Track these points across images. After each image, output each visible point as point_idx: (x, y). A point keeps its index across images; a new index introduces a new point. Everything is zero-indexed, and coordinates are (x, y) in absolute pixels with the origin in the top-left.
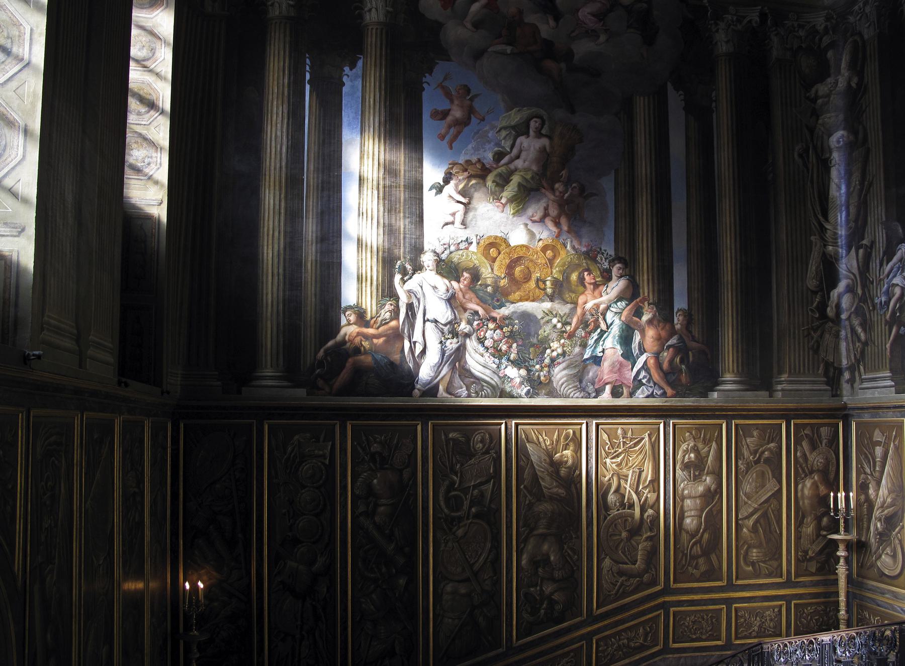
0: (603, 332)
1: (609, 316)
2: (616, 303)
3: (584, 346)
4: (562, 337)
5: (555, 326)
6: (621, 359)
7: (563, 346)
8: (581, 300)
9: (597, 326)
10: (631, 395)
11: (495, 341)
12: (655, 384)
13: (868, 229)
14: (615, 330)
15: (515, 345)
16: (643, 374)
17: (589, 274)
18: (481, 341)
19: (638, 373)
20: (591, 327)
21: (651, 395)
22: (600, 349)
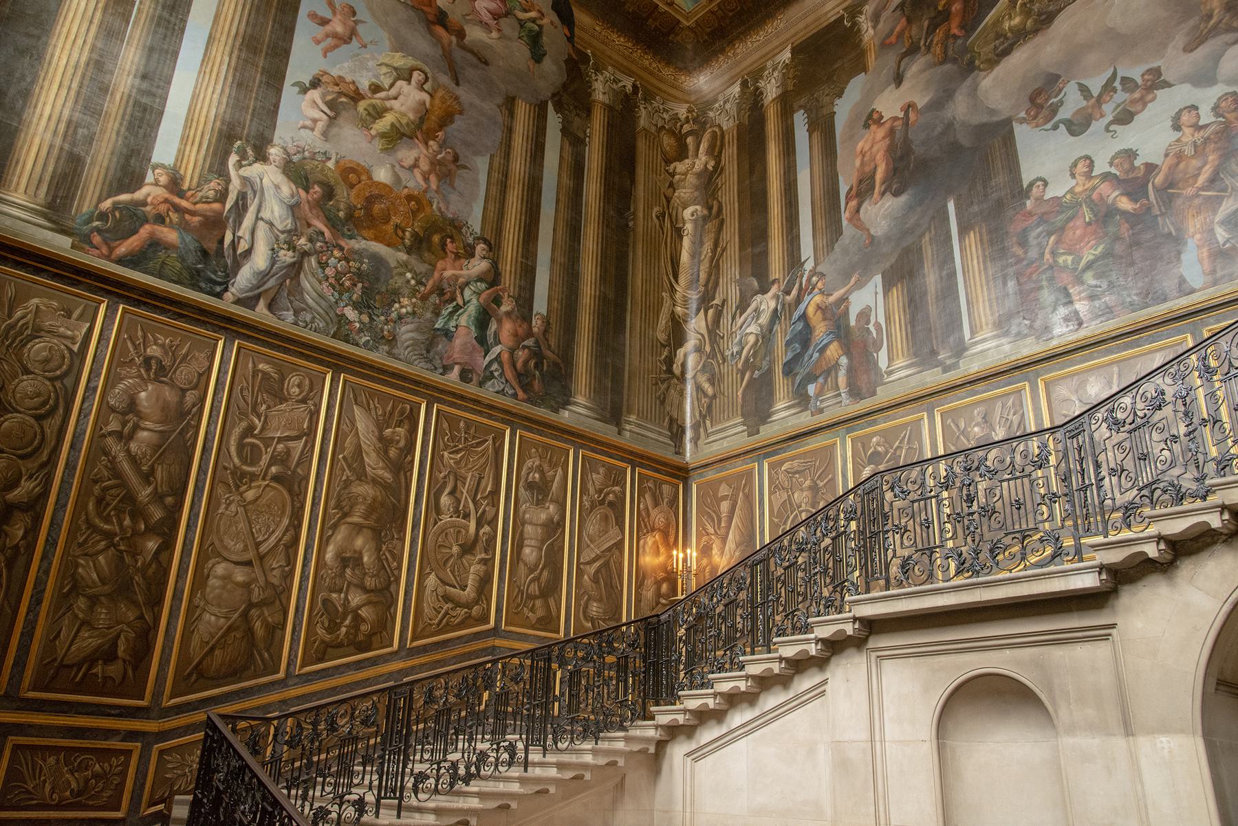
0: (458, 308)
1: (467, 293)
5: (408, 281)
8: (440, 265)
9: (453, 299)
11: (338, 272)
14: (472, 309)
15: (360, 285)
16: (495, 366)
18: (323, 265)
20: (447, 296)
21: (502, 392)
22: (453, 323)
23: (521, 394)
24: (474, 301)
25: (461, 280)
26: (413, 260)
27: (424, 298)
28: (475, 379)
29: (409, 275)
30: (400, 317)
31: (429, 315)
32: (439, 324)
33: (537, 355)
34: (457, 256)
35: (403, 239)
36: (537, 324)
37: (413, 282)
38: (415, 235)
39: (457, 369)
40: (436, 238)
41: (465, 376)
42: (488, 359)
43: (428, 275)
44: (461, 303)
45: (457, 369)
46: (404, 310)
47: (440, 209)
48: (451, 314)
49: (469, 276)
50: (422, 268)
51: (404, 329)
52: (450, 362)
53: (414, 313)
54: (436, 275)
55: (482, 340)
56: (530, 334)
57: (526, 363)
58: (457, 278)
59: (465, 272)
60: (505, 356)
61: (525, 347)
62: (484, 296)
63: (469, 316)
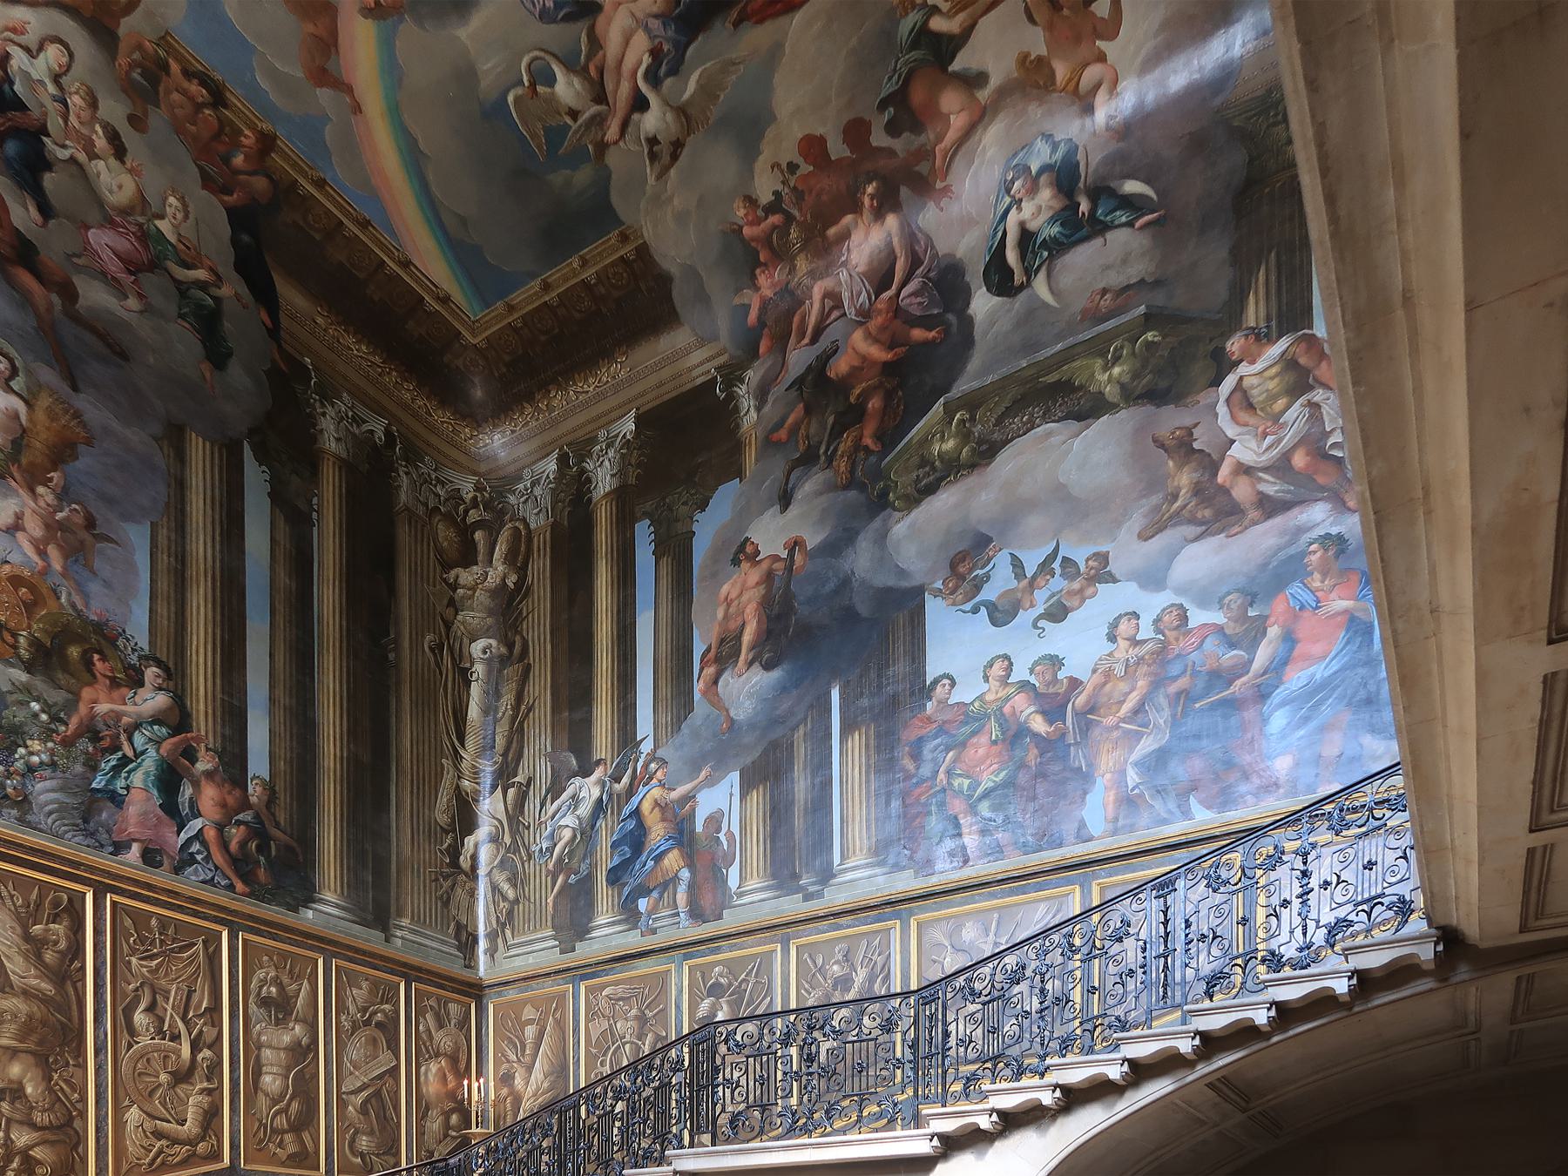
0: (125, 761)
1: (139, 739)
2: (152, 723)
3: (94, 769)
4: (49, 738)
5: (36, 716)
6: (161, 813)
7: (52, 753)
8: (87, 693)
9: (116, 748)
10: (177, 870)
12: (217, 868)
14: (149, 763)
16: (196, 847)
17: (104, 659)
19: (189, 842)
20: (106, 743)
21: (210, 882)
22: (120, 784)
23: (240, 886)
24: (152, 752)
25: (125, 720)
26: (39, 684)
27: (68, 743)
28: (166, 862)
29: (35, 706)
30: (31, 769)
31: (79, 768)
32: (98, 783)
33: (258, 832)
34: (114, 683)
35: (15, 647)
36: (255, 791)
37: (44, 717)
38: (35, 643)
39: (135, 847)
40: (74, 652)
41: (151, 857)
42: (183, 836)
43: (72, 705)
44: (130, 754)
45: (135, 847)
46: (35, 759)
47: (73, 606)
48: (117, 770)
49: (139, 715)
50: (57, 697)
51: (39, 786)
52: (123, 837)
53: (53, 765)
54: (83, 709)
55: (170, 807)
56: (245, 805)
57: (243, 844)
58: (118, 716)
59: (129, 708)
60: (211, 834)
61: (239, 823)
62: (167, 746)
63: (147, 774)
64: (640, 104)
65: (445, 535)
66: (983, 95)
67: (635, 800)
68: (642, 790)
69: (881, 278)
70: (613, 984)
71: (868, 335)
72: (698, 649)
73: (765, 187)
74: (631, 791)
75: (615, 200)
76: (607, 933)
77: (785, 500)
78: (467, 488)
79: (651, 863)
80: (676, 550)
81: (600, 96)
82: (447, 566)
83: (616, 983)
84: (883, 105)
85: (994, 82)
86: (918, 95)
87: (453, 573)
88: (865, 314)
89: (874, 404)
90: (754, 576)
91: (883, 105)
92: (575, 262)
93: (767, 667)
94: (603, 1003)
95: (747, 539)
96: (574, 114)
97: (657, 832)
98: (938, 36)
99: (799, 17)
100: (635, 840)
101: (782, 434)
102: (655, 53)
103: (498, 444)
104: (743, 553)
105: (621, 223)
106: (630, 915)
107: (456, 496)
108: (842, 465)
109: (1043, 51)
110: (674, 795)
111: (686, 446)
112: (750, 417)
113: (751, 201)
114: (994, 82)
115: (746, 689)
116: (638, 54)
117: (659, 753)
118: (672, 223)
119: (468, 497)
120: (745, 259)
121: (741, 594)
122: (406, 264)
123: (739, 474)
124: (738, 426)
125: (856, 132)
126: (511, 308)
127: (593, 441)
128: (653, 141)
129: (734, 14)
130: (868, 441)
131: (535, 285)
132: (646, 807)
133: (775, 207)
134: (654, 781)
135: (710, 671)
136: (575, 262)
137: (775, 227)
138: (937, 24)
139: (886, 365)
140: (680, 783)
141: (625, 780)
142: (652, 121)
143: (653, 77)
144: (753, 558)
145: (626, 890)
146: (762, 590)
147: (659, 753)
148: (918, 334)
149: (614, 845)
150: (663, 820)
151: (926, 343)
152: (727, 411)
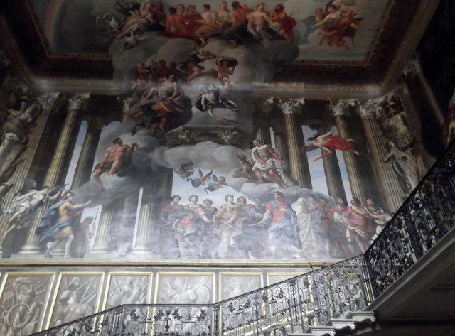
13: (12, 178)
64: (129, 35)
65: (12, 99)
66: (203, 72)
67: (57, 205)
68: (61, 202)
69: (170, 93)
70: (23, 277)
71: (164, 104)
72: (96, 163)
73: (148, 64)
74: (56, 201)
75: (110, 49)
76: (28, 253)
77: (134, 132)
78: (25, 89)
79: (57, 229)
80: (94, 134)
81: (120, 28)
82: (9, 107)
83: (24, 276)
84: (182, 63)
85: (205, 71)
86: (190, 65)
87: (9, 111)
88: (163, 100)
89: (164, 119)
90: (120, 149)
91: (182, 63)
92: (91, 55)
93: (119, 176)
94: (14, 284)
95: (119, 138)
96: (111, 29)
97: (64, 218)
98: (198, 58)
99: (172, 40)
100: (55, 217)
101: (136, 116)
102: (138, 29)
103: (44, 84)
104: (117, 141)
105: (108, 53)
106: (42, 248)
107: (21, 90)
108: (153, 130)
109: (217, 70)
110: (75, 207)
111: (103, 110)
112: (126, 108)
113: (143, 65)
114: (205, 71)
115: (110, 180)
116: (135, 27)
117: (72, 191)
118: (120, 60)
119: (24, 92)
120: (136, 74)
121: (114, 152)
122: (42, 32)
123: (121, 121)
124: (123, 110)
125: (173, 64)
126: (65, 55)
127: (74, 95)
128: (127, 43)
129: (160, 32)
130: (161, 127)
131: (76, 54)
132: (62, 208)
133: (149, 68)
134: (68, 200)
135: (99, 170)
136: (91, 55)
137: (146, 72)
138: (198, 55)
139: (168, 113)
140: (78, 203)
141: (55, 196)
142: (129, 39)
143: (135, 33)
144: (121, 143)
145: (44, 237)
146: (122, 153)
147: (72, 191)
148: (177, 109)
149: (43, 219)
150: (67, 214)
151: (178, 111)
152: (121, 105)
